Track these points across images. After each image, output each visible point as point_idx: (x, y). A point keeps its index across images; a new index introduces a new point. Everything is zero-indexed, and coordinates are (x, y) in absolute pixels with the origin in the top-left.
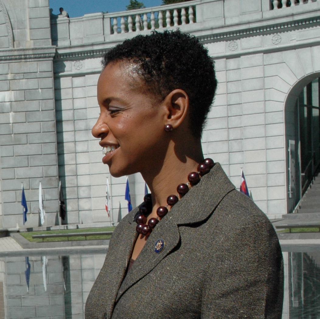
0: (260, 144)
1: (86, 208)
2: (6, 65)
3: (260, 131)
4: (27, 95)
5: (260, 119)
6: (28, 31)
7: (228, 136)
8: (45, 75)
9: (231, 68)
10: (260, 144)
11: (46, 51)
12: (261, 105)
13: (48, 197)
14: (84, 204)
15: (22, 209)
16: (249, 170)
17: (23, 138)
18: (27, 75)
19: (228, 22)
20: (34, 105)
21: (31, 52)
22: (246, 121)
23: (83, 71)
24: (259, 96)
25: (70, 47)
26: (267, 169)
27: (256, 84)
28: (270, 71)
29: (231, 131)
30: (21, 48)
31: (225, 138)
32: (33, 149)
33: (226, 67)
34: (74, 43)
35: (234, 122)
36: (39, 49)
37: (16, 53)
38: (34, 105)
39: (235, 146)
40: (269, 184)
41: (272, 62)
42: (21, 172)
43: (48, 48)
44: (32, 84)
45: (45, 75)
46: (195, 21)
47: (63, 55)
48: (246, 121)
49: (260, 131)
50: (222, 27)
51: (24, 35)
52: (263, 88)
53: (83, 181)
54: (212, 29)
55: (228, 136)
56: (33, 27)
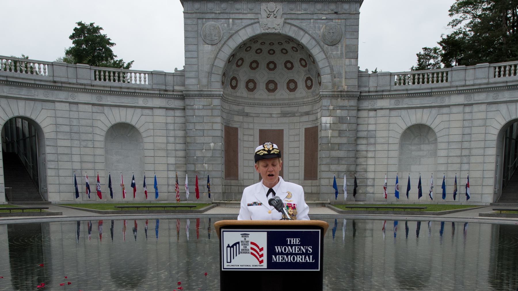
0: (480, 159)
1: (371, 192)
2: (329, 101)
3: (481, 152)
4: (341, 120)
5: (482, 144)
6: (344, 80)
7: (461, 154)
8: (352, 108)
9: (467, 112)
10: (480, 159)
11: (354, 93)
12: (483, 136)
13: (348, 184)
14: (370, 189)
15: (334, 191)
16: (473, 175)
17: (336, 147)
18: (342, 108)
19: (468, 83)
20: (344, 127)
21: (345, 93)
22: (473, 144)
23: (376, 107)
24: (482, 130)
25: (369, 92)
26: (483, 175)
27: (481, 122)
28: (490, 115)
29: (463, 150)
30: (339, 90)
31: (459, 154)
32: (341, 154)
33: (463, 111)
34: (372, 89)
35: (466, 145)
36: (350, 91)
37: (336, 93)
38: (344, 127)
39: (465, 160)
40: (484, 184)
41: (492, 110)
42: (333, 167)
43: (355, 92)
44: (344, 113)
45: (352, 108)
46: (447, 81)
47: (364, 96)
48: (473, 144)
49: (481, 152)
50: (464, 86)
51: (341, 82)
52: (485, 125)
53: (370, 175)
54: (457, 87)
55: (461, 154)
56: (347, 77)
